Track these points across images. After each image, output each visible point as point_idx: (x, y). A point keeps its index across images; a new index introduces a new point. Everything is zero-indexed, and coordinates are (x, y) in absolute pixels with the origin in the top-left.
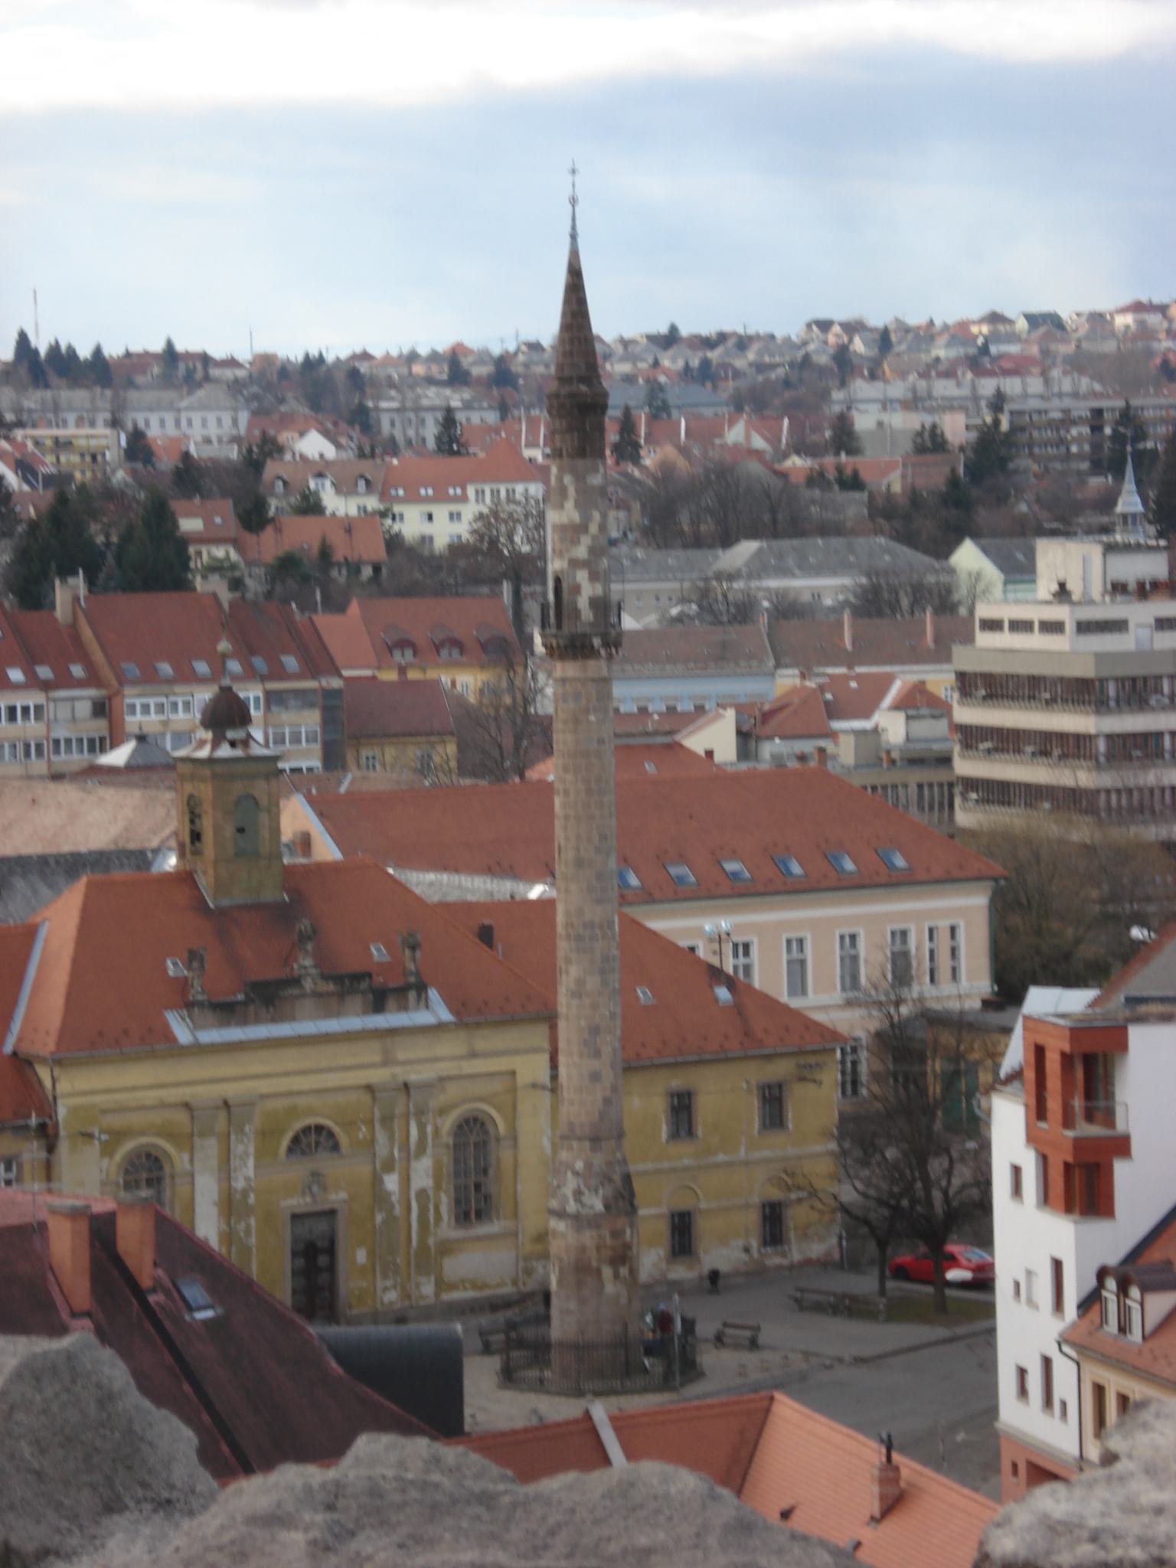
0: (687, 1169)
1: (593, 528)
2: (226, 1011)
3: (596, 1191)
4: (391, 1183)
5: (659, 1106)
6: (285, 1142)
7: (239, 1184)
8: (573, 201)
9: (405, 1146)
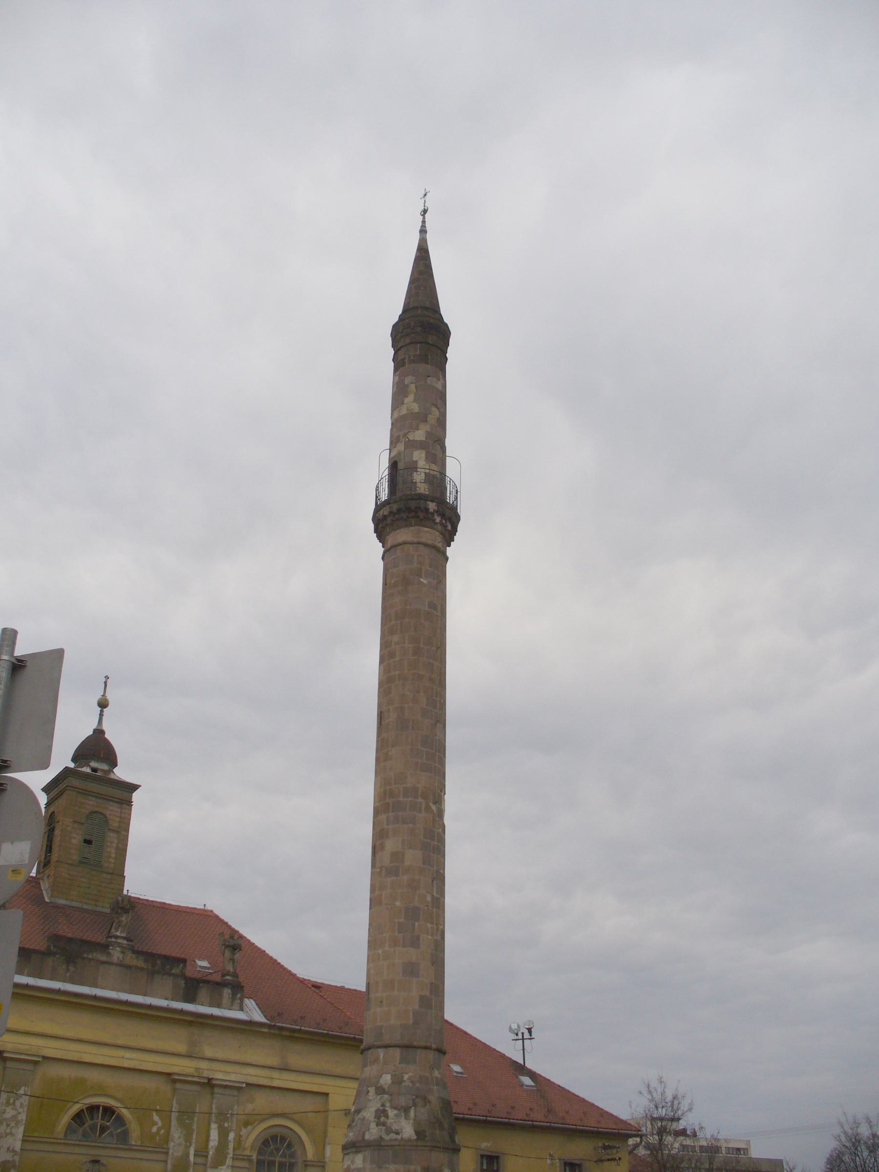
3: (406, 1110)
6: (66, 1119)
9: (202, 1153)
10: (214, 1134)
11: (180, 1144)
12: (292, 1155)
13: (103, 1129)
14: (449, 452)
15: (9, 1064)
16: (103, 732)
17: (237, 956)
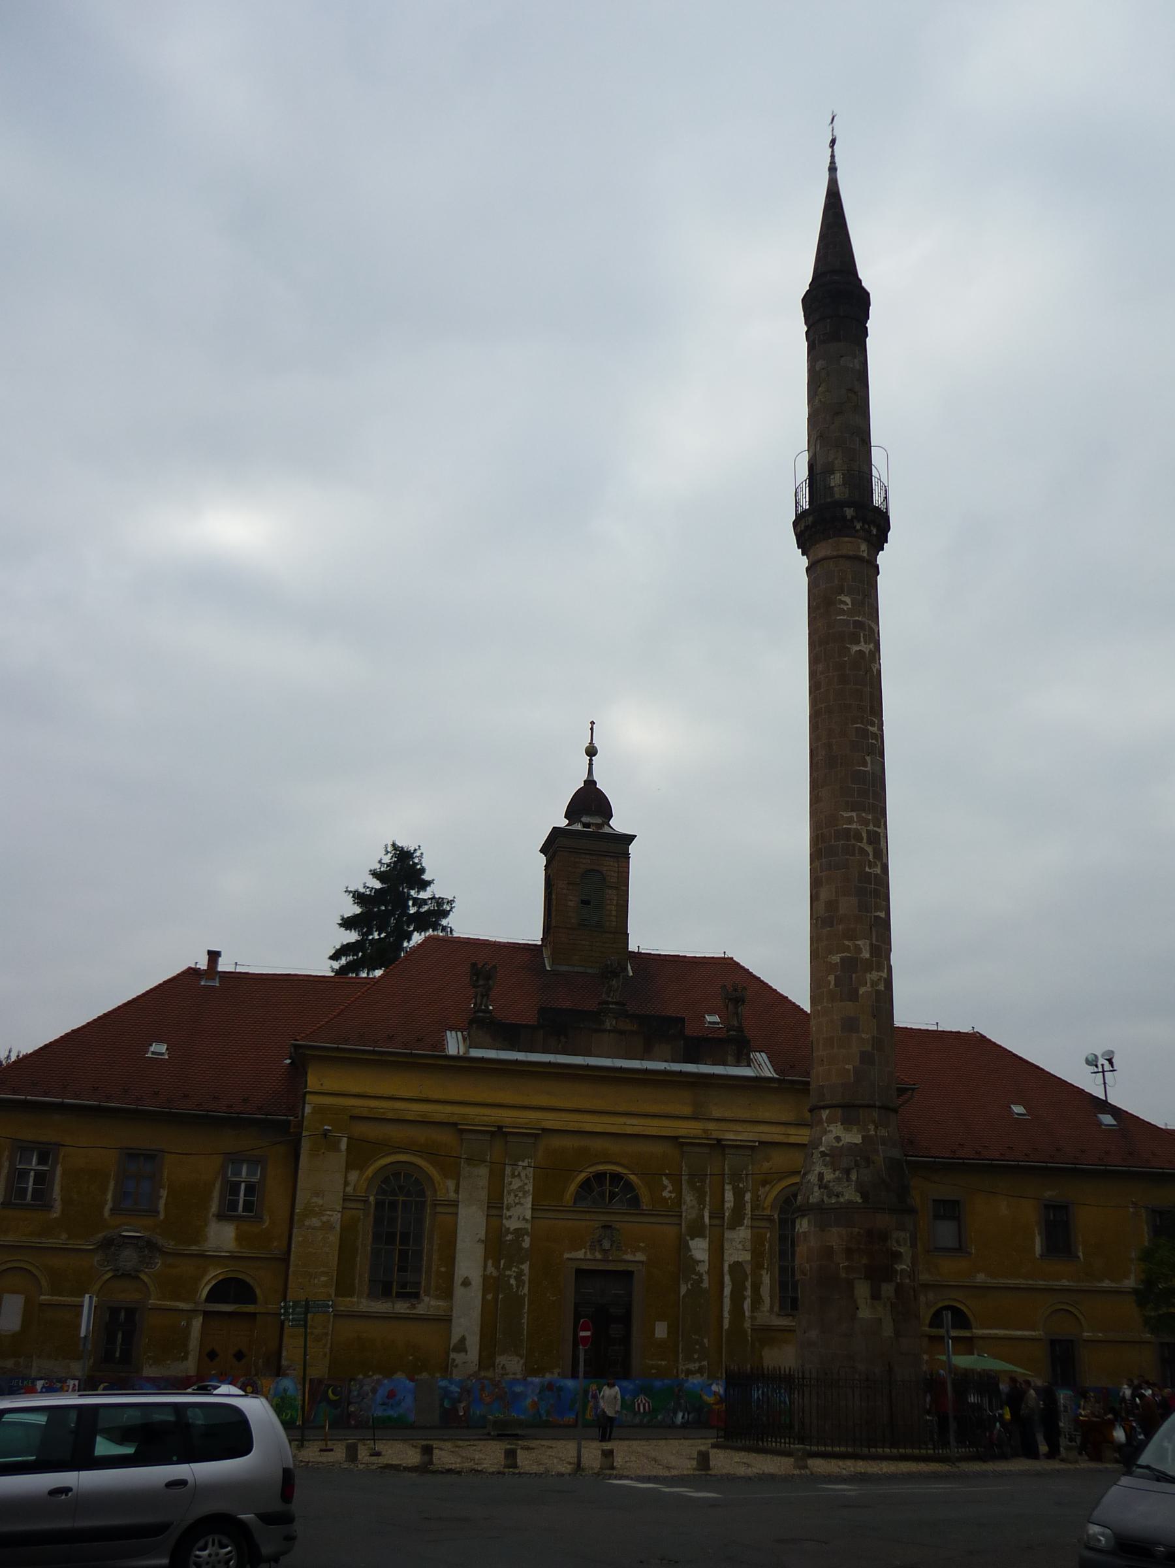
0: (1068, 1290)
2: (509, 1035)
3: (847, 1172)
4: (699, 1249)
6: (573, 1187)
7: (513, 1224)
9: (717, 1214)
10: (729, 1196)
11: (693, 1207)
13: (613, 1195)
14: (874, 440)
16: (595, 783)
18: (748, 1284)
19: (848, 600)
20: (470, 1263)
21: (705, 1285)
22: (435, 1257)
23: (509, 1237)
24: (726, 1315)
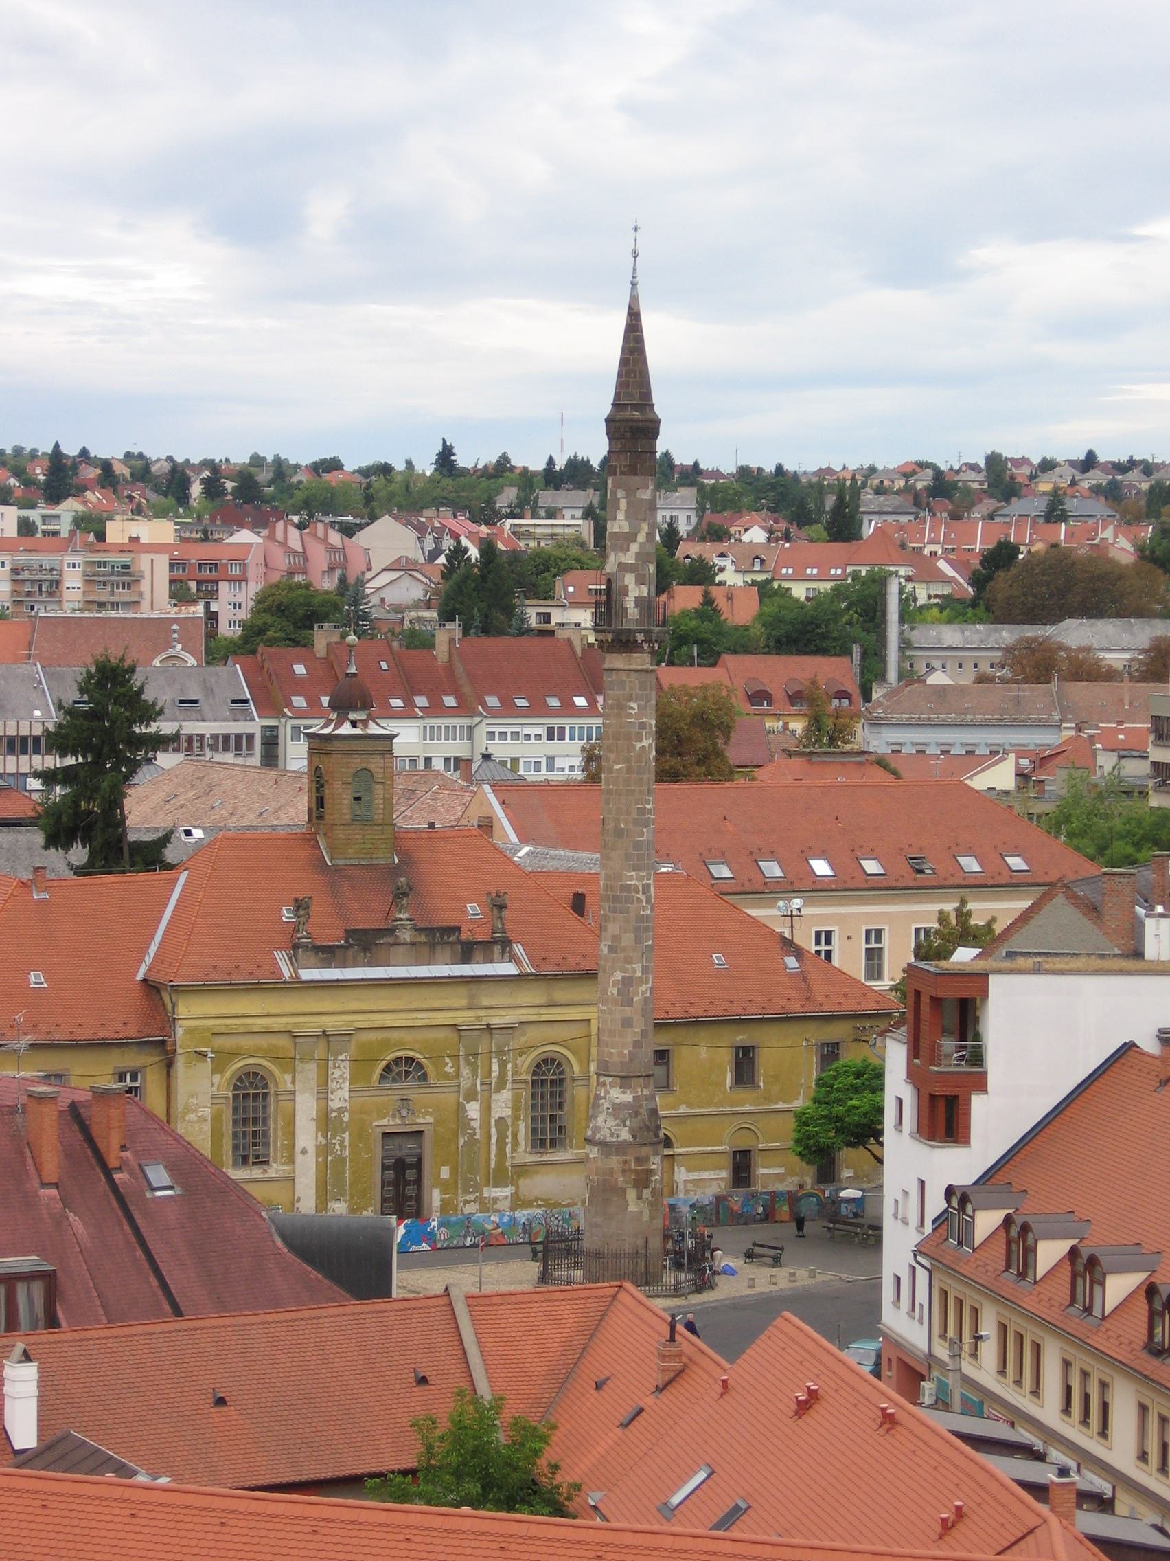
1: (641, 538)
2: (328, 954)
4: (473, 1110)
5: (726, 1058)
6: (378, 1071)
7: (334, 1105)
8: (635, 255)
9: (486, 1083)
12: (562, 1073)
15: (331, 1039)
17: (505, 913)
18: (509, 1133)
19: (634, 705)
20: (306, 1137)
21: (477, 1137)
22: (280, 1133)
23: (334, 1114)
24: (493, 1157)
